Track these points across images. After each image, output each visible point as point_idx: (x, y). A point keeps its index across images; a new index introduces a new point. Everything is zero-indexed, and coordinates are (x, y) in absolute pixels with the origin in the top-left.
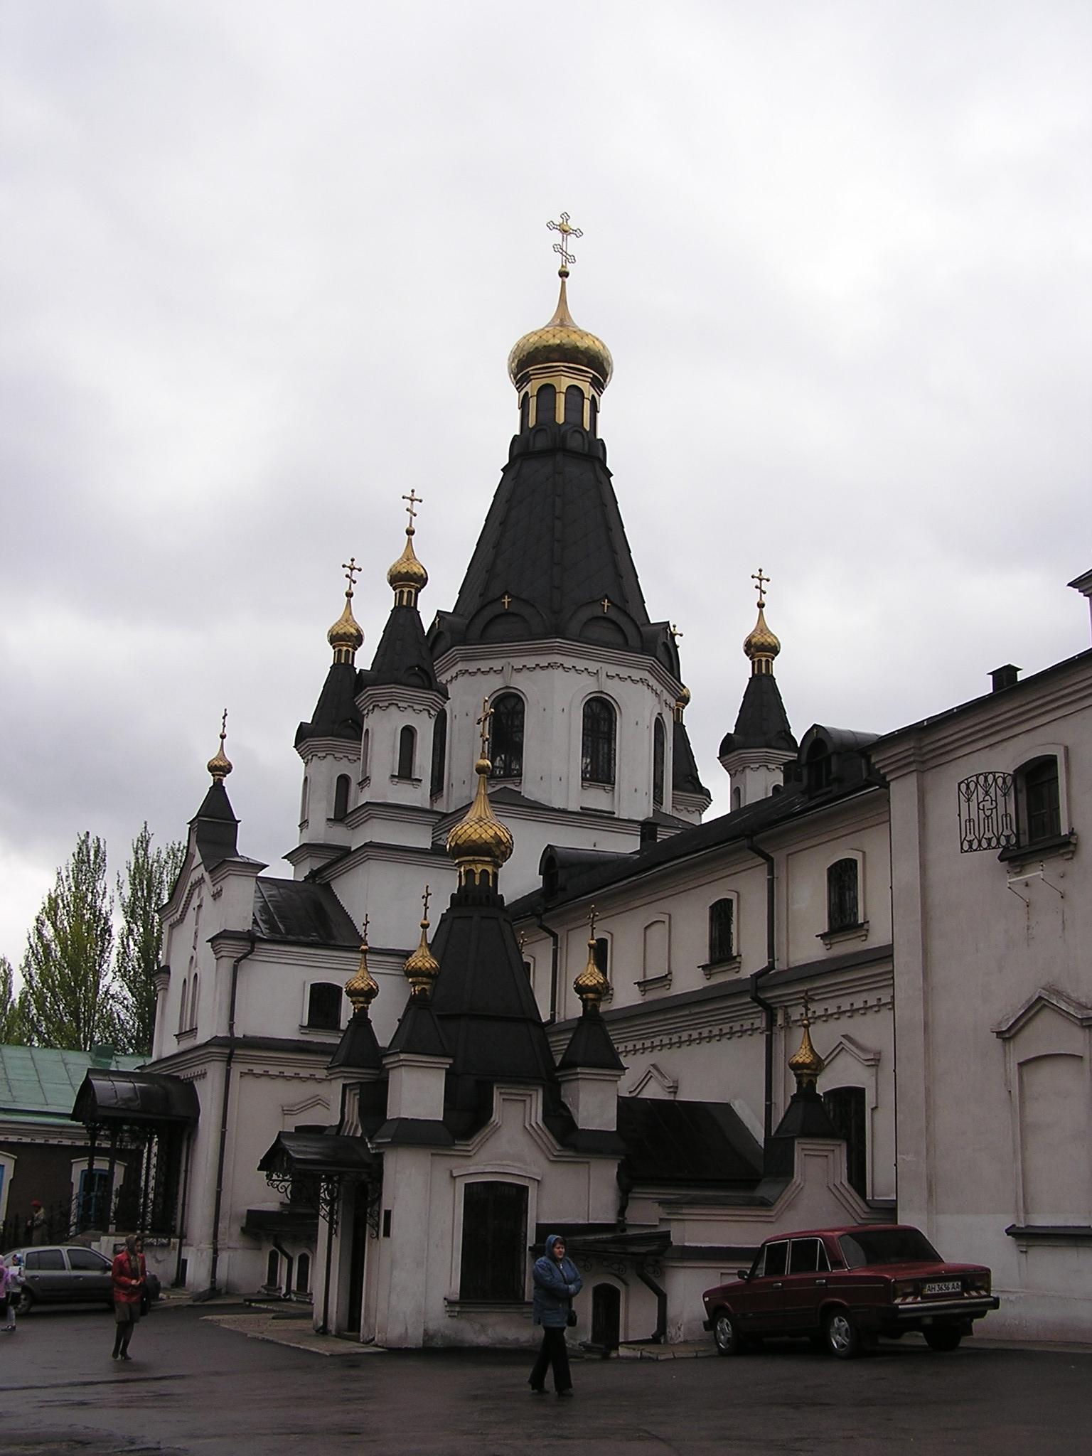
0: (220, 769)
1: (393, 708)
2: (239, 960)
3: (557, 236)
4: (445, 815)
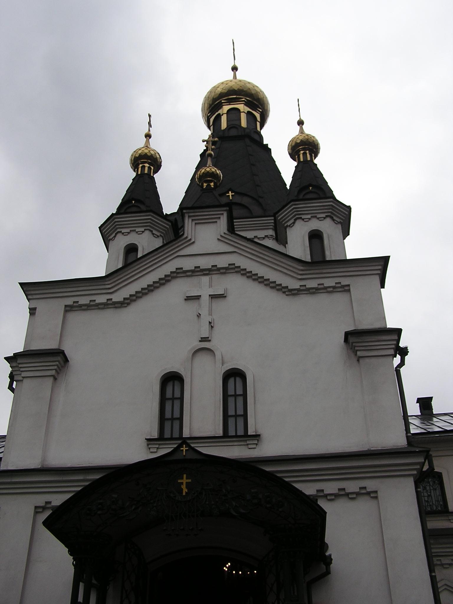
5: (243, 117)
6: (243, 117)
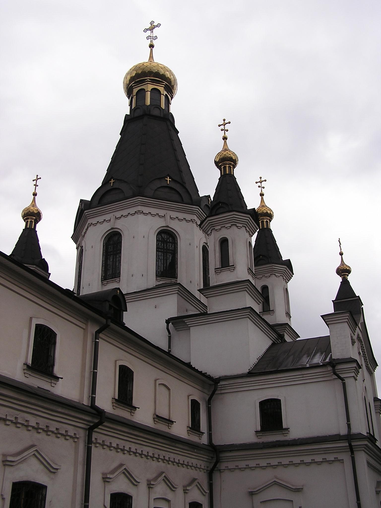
5: (148, 94)
6: (148, 94)
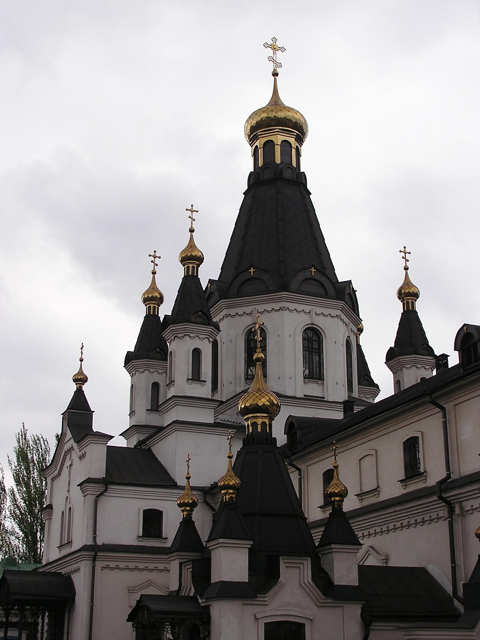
0: (80, 379)
1: (187, 338)
2: (98, 496)
3: (270, 52)
4: (222, 403)
5: (278, 149)
6: (278, 149)
